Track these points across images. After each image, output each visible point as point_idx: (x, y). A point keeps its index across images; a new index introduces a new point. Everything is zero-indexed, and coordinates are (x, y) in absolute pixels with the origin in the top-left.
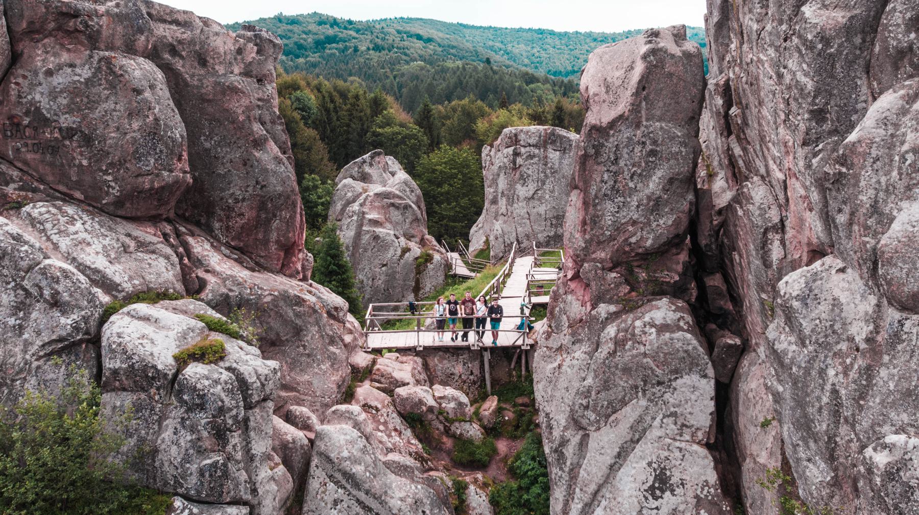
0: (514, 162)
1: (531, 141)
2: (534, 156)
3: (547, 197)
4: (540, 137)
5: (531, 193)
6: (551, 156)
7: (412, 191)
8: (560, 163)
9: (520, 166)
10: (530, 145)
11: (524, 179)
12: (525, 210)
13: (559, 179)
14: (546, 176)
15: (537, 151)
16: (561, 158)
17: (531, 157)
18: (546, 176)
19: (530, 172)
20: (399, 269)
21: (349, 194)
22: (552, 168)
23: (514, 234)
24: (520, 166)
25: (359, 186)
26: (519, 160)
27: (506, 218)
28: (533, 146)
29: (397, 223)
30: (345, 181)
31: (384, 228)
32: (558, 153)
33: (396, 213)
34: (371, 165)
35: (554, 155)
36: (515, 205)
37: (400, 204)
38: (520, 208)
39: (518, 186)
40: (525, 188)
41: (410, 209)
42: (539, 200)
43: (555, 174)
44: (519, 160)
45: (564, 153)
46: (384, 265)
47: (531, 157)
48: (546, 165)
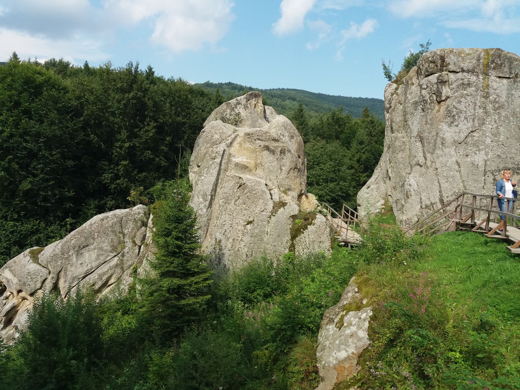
0: (438, 93)
1: (466, 65)
2: (469, 85)
3: (488, 141)
4: (478, 60)
5: (463, 136)
6: (495, 85)
7: (292, 137)
8: (510, 95)
9: (448, 97)
10: (463, 71)
11: (452, 117)
12: (454, 159)
13: (506, 117)
14: (486, 113)
15: (473, 78)
16: (509, 90)
17: (466, 85)
18: (486, 113)
19: (462, 107)
20: (268, 229)
21: (217, 136)
22: (495, 101)
24: (448, 97)
25: (229, 128)
26: (446, 91)
27: (423, 169)
28: (468, 71)
29: (270, 171)
30: (214, 123)
31: (254, 175)
32: (505, 81)
33: (271, 157)
34: (246, 107)
35: (499, 86)
36: (438, 152)
37: (276, 147)
38: (449, 156)
39: (444, 127)
40: (454, 129)
41: (288, 155)
42: (475, 144)
44: (446, 91)
45: (515, 82)
46: (249, 223)
47: (466, 85)
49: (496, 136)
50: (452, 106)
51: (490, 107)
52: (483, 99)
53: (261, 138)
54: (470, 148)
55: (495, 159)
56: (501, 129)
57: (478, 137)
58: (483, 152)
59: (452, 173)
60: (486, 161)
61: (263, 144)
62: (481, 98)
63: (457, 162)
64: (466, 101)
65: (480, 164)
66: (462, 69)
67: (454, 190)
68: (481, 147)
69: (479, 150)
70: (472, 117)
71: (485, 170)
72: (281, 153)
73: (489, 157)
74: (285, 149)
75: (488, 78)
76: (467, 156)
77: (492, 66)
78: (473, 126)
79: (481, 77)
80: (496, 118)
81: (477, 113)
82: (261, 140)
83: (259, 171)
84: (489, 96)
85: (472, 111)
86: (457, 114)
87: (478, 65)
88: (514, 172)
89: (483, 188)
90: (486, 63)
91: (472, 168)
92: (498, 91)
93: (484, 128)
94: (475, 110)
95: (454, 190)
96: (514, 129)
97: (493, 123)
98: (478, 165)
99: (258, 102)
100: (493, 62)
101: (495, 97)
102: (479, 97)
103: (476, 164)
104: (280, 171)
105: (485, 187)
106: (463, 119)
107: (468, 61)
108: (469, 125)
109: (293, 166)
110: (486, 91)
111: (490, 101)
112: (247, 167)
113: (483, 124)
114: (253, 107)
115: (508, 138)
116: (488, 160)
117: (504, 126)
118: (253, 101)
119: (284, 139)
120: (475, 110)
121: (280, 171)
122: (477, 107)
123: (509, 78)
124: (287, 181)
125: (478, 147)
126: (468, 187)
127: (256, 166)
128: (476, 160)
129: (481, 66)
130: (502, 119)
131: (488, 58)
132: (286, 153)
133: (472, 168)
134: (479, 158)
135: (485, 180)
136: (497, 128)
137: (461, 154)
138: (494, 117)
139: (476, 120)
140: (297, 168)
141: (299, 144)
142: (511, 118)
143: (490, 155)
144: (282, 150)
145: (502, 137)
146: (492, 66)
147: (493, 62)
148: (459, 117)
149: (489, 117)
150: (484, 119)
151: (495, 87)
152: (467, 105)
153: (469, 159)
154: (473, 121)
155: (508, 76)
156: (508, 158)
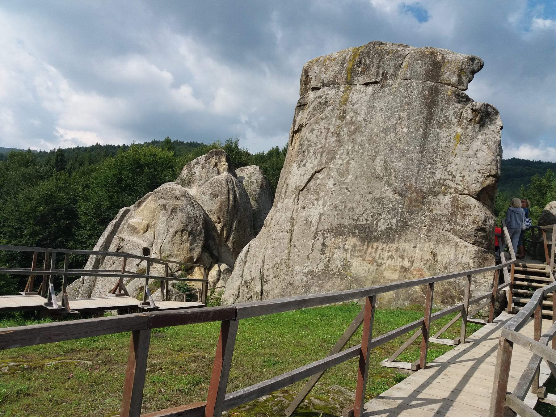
1: (326, 76)
7: (216, 196)
10: (324, 85)
14: (340, 142)
15: (331, 92)
22: (352, 123)
31: (140, 237)
32: (371, 88)
34: (204, 166)
40: (302, 169)
48: (342, 118)
49: (343, 176)
50: (305, 138)
52: (339, 121)
55: (330, 213)
56: (353, 164)
57: (322, 179)
58: (321, 202)
60: (321, 215)
61: (162, 201)
62: (336, 121)
64: (320, 127)
65: (313, 220)
66: (323, 82)
67: (276, 259)
68: (322, 194)
69: (317, 200)
70: (321, 150)
71: (316, 229)
72: (172, 212)
73: (325, 209)
74: (177, 208)
75: (351, 89)
76: (304, 208)
78: (320, 163)
79: (342, 89)
80: (350, 148)
81: (329, 143)
82: (165, 199)
83: (149, 234)
84: (345, 116)
85: (323, 141)
86: (307, 148)
87: (340, 73)
88: (349, 233)
89: (308, 258)
90: (350, 67)
91: (304, 227)
92: (358, 105)
93: (331, 166)
94: (326, 139)
95: (276, 259)
96: (366, 164)
97: (345, 156)
98: (311, 221)
99: (220, 161)
100: (360, 63)
101: (352, 115)
102: (334, 119)
103: (310, 220)
104: (166, 234)
105: (310, 256)
106: (311, 154)
107: (331, 69)
108: (316, 163)
109: (180, 229)
110: (342, 108)
111: (346, 123)
112: (136, 229)
113: (333, 158)
114: (212, 166)
116: (323, 214)
117: (356, 159)
118: (214, 160)
119: (204, 197)
120: (326, 139)
121: (166, 234)
122: (330, 134)
123: (375, 83)
124: (170, 245)
125: (318, 194)
126: (292, 255)
127: (147, 228)
128: (312, 214)
129: (344, 73)
130: (356, 147)
131: (354, 59)
132: (178, 212)
133: (304, 227)
134: (314, 213)
135: (313, 244)
136: (348, 163)
137: (300, 205)
138: (347, 147)
139: (325, 154)
140: (187, 231)
141: (221, 204)
142: (367, 145)
143: (327, 206)
144: (173, 209)
145: (350, 176)
146: (360, 69)
147: (360, 63)
148: (309, 152)
149: (342, 148)
150: (335, 152)
151: (355, 100)
152: (320, 132)
153: (304, 214)
154: (321, 156)
155: (373, 80)
156: (347, 210)
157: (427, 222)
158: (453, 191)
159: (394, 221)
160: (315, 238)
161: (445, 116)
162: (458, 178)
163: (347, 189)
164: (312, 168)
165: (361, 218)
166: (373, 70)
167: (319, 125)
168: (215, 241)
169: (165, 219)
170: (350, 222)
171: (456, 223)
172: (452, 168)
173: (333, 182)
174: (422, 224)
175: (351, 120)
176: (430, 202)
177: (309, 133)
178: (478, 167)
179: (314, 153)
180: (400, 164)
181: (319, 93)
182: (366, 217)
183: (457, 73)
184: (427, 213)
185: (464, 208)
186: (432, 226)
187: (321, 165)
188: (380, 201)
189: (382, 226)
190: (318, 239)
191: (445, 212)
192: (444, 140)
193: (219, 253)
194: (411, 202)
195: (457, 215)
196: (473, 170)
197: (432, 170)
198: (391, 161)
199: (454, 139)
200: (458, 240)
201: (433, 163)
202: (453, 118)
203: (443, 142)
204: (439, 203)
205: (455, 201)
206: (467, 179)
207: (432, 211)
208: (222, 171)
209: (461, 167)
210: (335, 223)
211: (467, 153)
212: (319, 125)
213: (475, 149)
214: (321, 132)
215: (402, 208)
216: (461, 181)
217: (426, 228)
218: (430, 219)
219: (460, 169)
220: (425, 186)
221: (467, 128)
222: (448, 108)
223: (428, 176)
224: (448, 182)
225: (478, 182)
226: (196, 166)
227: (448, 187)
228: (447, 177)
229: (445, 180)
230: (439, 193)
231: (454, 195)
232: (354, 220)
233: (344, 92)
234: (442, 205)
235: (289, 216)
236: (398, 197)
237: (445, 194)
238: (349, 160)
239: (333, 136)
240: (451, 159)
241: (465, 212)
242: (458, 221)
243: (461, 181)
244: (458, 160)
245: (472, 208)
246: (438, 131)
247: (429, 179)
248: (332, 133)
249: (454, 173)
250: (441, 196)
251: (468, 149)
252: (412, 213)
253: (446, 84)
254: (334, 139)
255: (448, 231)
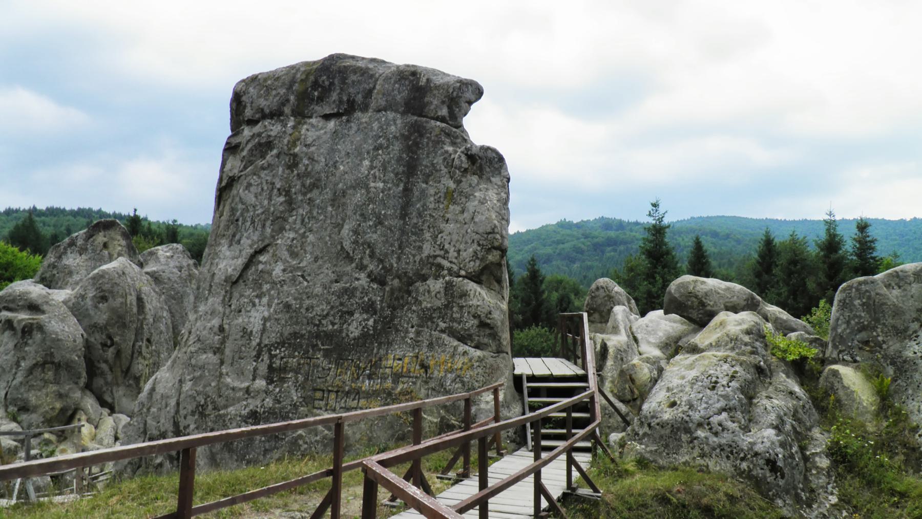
4: (290, 88)
7: (104, 299)
10: (264, 117)
12: (216, 322)
14: (290, 204)
15: (275, 128)
23: (173, 402)
32: (332, 124)
43: (314, 194)
51: (297, 186)
52: (287, 172)
53: (11, 305)
54: (247, 293)
56: (311, 238)
58: (265, 300)
59: (204, 356)
60: (265, 320)
62: (283, 172)
63: (221, 329)
65: (255, 330)
66: (262, 110)
68: (266, 287)
69: (259, 297)
71: (259, 344)
73: (272, 310)
76: (240, 311)
77: (316, 94)
79: (290, 124)
81: (274, 205)
85: (266, 202)
86: (242, 215)
91: (240, 343)
94: (270, 199)
96: (330, 237)
98: (251, 332)
101: (307, 162)
102: (281, 169)
104: (14, 371)
107: (274, 92)
111: (298, 175)
115: (316, 259)
120: (270, 199)
122: (275, 191)
128: (252, 320)
130: (315, 214)
132: (35, 332)
134: (255, 318)
137: (233, 307)
139: (268, 223)
140: (53, 363)
142: (330, 209)
146: (316, 94)
148: (245, 221)
149: (294, 213)
154: (264, 226)
156: (303, 311)
157: (415, 320)
158: (446, 272)
159: (371, 322)
160: (258, 358)
161: (433, 164)
162: (452, 254)
163: (303, 276)
164: (251, 246)
165: (324, 322)
166: (334, 96)
167: (259, 177)
168: (105, 379)
169: (11, 345)
170: (309, 329)
171: (453, 320)
172: (444, 237)
173: (282, 267)
174: (408, 324)
175: (306, 169)
176: (417, 290)
177: (244, 191)
178: (476, 237)
179: (253, 222)
180: (375, 236)
181: (257, 129)
182: (331, 318)
183: (448, 103)
184: (414, 308)
185: (461, 297)
186: (422, 327)
187: (263, 240)
188: (349, 292)
189: (354, 330)
190: (262, 360)
191: (438, 303)
192: (432, 199)
193: (113, 399)
194: (392, 291)
195: (453, 307)
196: (470, 241)
197: (418, 244)
198: (364, 232)
199: (445, 198)
200: (456, 343)
201: (419, 232)
202: (443, 168)
203: (431, 202)
204: (429, 292)
205: (449, 286)
206: (464, 254)
207: (420, 303)
208: (116, 256)
209: (455, 237)
210: (288, 331)
211: (461, 218)
212: (259, 177)
213: (471, 209)
214: (262, 189)
215: (382, 301)
216: (456, 258)
217: (414, 330)
218: (418, 316)
219: (454, 240)
220: (410, 267)
221: (461, 181)
222: (436, 153)
223: (413, 252)
224: (439, 260)
225: (478, 258)
226: (69, 251)
227: (440, 267)
228: (438, 252)
229: (435, 257)
230: (429, 276)
231: (447, 278)
232: (315, 325)
233: (294, 127)
234: (433, 294)
235: (217, 325)
236: (375, 286)
237: (437, 277)
238: (305, 232)
239: (280, 194)
240: (443, 225)
241: (462, 302)
242: (454, 316)
243: (456, 258)
244: (451, 226)
245: (472, 296)
246: (424, 185)
247: (414, 256)
248: (279, 190)
249: (447, 246)
250: (430, 282)
251: (463, 212)
252: (395, 309)
253: (433, 118)
254: (282, 199)
255: (443, 331)
